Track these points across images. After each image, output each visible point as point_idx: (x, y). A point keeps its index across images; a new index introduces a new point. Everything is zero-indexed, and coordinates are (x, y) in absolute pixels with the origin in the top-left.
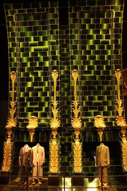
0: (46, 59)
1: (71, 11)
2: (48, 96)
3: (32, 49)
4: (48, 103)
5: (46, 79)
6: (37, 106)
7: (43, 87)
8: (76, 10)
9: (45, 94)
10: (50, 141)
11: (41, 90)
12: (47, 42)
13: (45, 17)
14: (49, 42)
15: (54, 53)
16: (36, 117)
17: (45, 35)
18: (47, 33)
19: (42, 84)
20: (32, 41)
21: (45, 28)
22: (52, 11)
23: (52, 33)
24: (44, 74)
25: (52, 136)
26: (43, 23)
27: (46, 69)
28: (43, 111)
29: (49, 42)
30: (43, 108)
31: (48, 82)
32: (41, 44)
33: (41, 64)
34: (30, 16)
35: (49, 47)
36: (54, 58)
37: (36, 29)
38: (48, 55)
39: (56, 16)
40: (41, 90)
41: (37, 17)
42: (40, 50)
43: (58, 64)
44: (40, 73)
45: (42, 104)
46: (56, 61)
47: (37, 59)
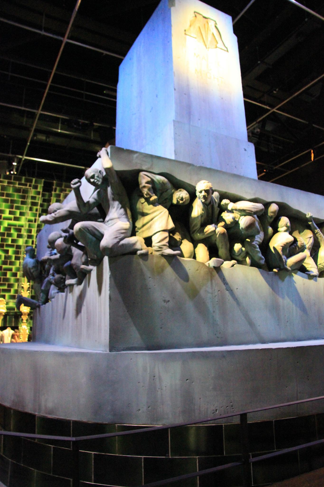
0: (20, 236)
1: (55, 191)
2: (18, 277)
3: (6, 223)
4: (18, 285)
5: (17, 258)
6: (6, 287)
7: (14, 268)
8: (62, 191)
9: (15, 275)
10: (20, 325)
11: (11, 270)
12: (23, 218)
13: (26, 191)
14: (26, 218)
15: (30, 231)
16: (4, 300)
17: (23, 209)
18: (25, 208)
19: (12, 263)
20: (7, 214)
21: (23, 203)
22: (36, 187)
23: (31, 209)
24: (17, 253)
25: (22, 320)
26: (23, 197)
27: (19, 247)
28: (12, 293)
29: (26, 218)
30: (12, 290)
31: (20, 263)
32: (16, 219)
33: (13, 241)
34: (9, 187)
35: (26, 224)
36: (30, 237)
37: (13, 201)
38: (24, 233)
39: (38, 193)
40: (11, 270)
41: (18, 190)
42: (15, 225)
43: (33, 243)
44: (11, 251)
45: (10, 286)
46: (30, 240)
47: (10, 235)
